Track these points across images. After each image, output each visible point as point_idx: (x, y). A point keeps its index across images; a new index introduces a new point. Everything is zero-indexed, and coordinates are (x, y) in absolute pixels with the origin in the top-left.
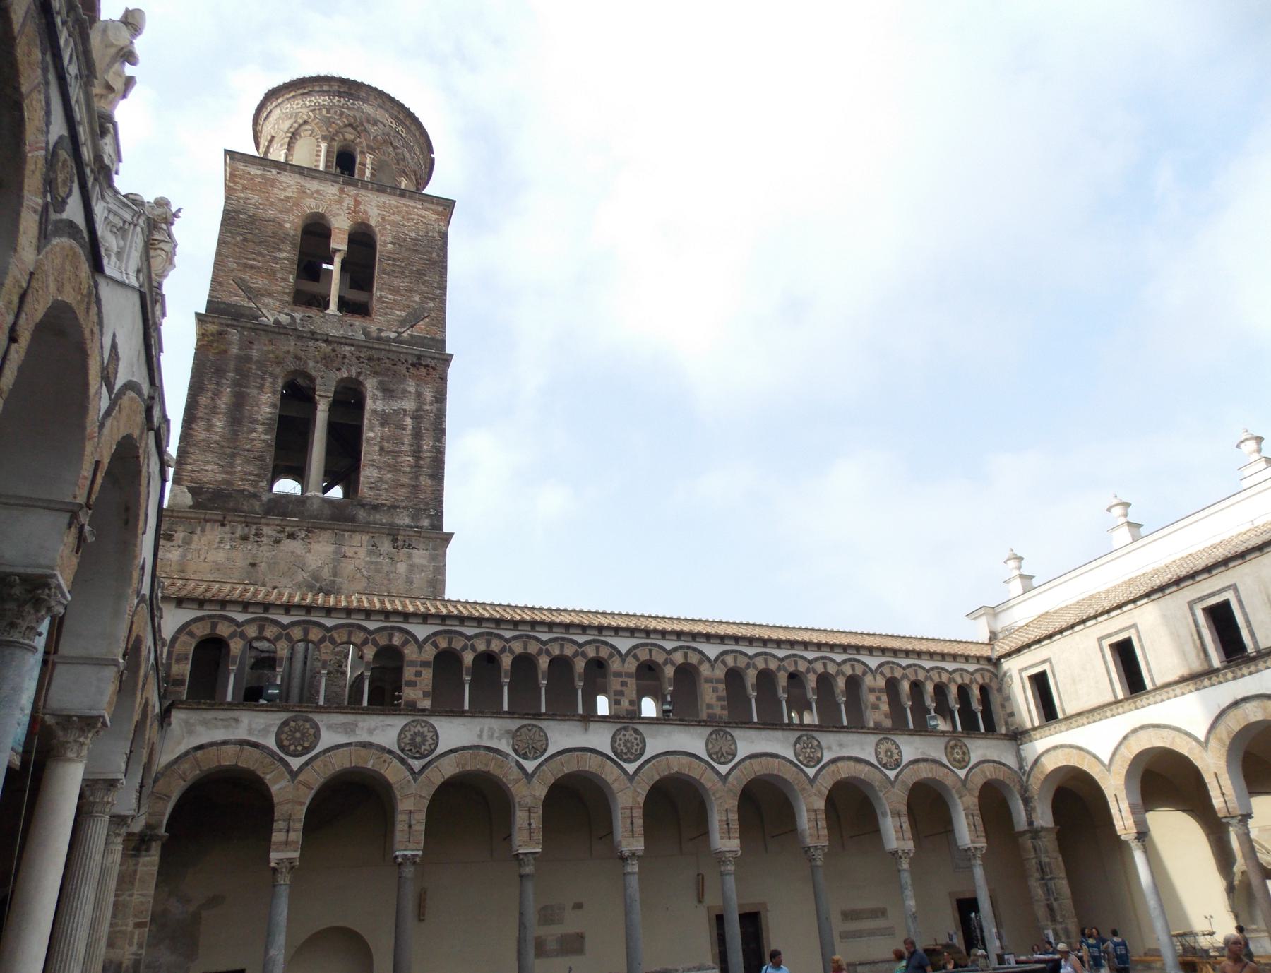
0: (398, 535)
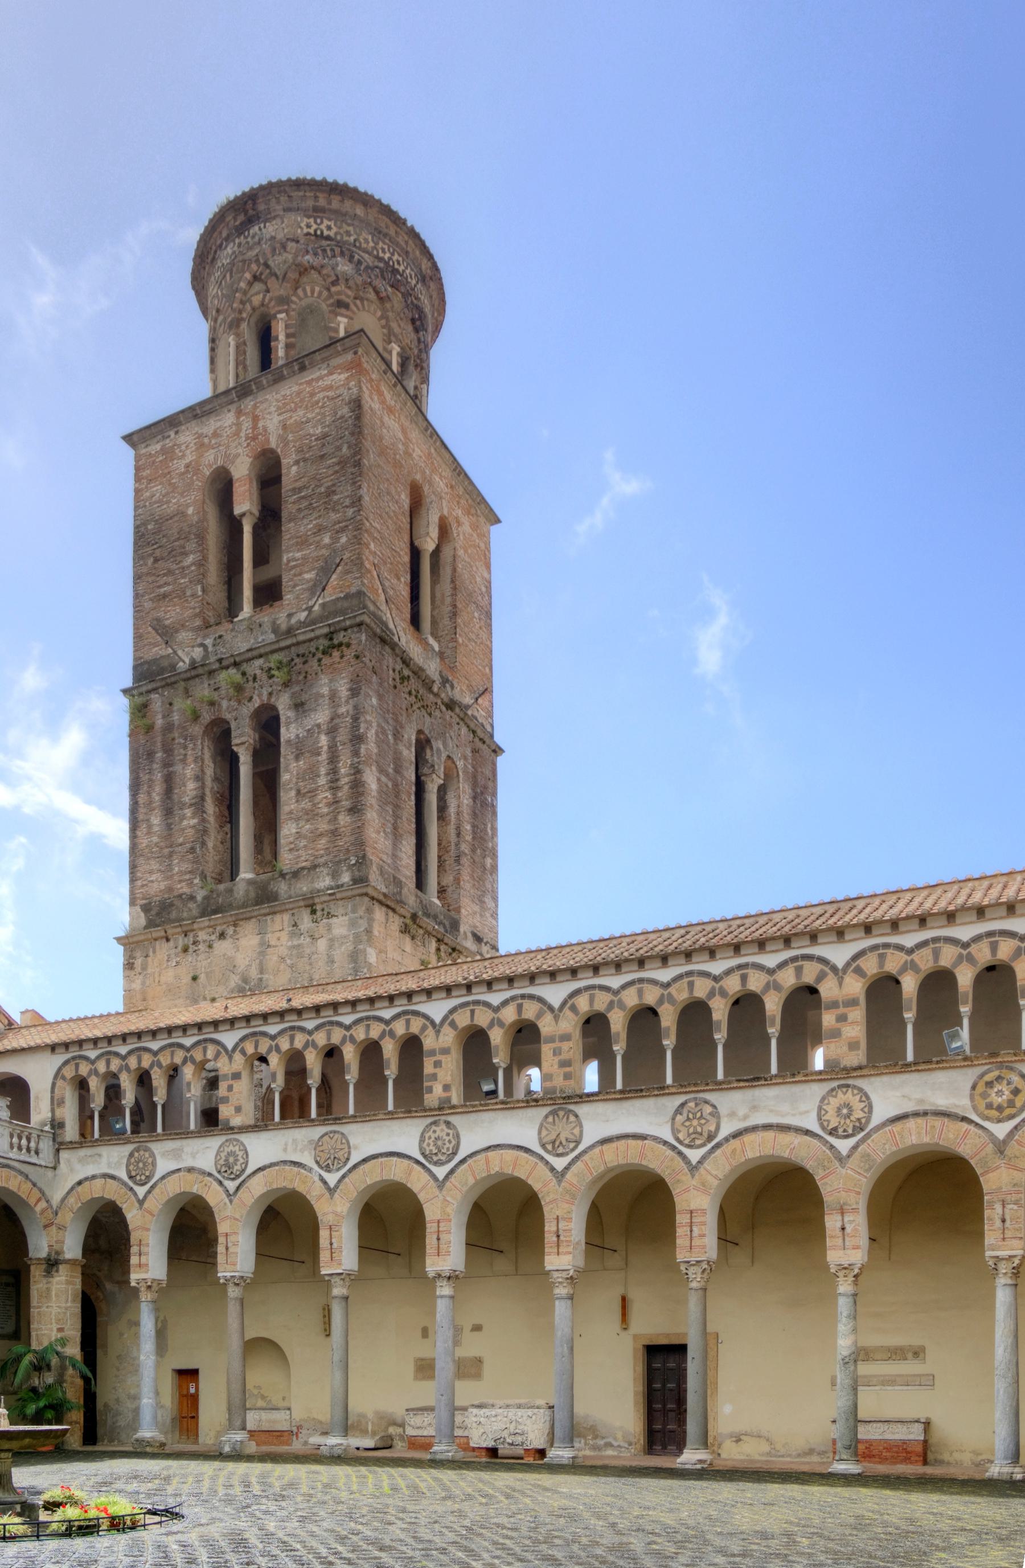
0: (314, 904)
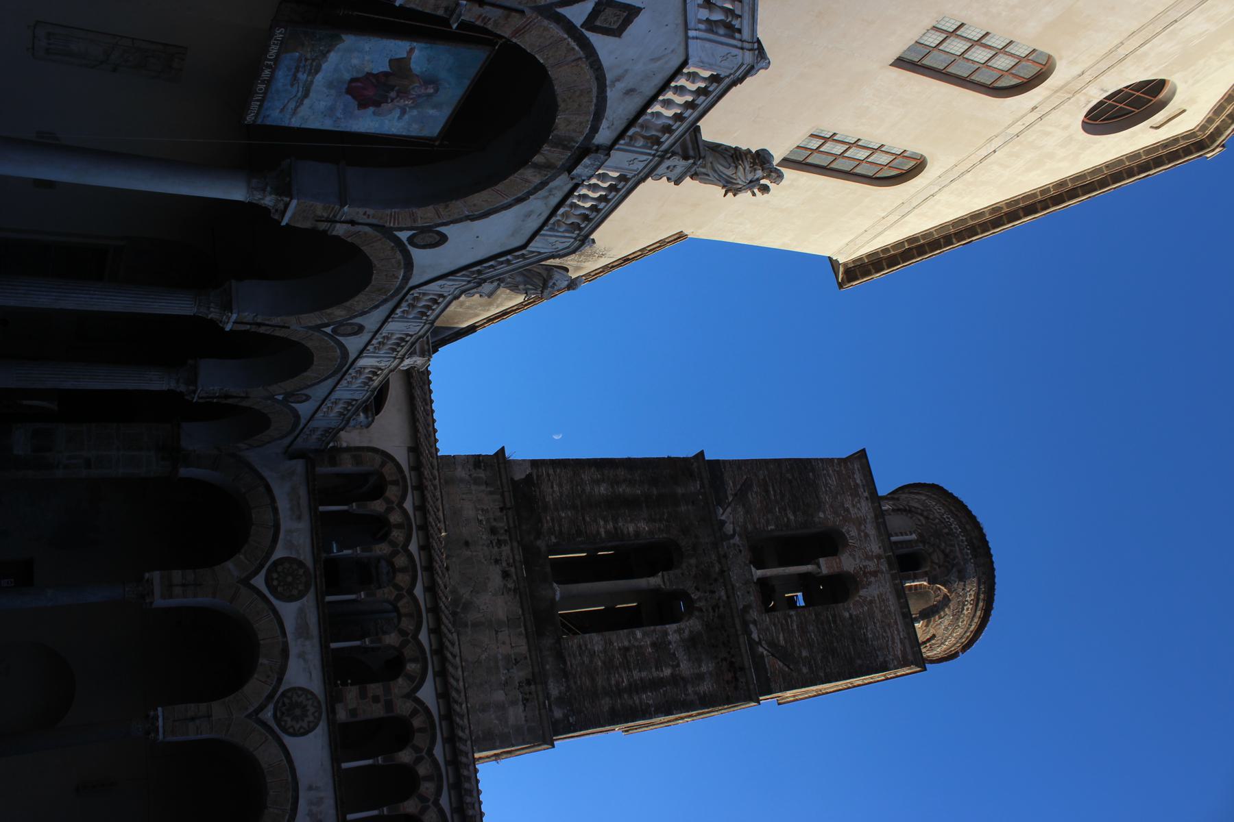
0: (535, 684)
